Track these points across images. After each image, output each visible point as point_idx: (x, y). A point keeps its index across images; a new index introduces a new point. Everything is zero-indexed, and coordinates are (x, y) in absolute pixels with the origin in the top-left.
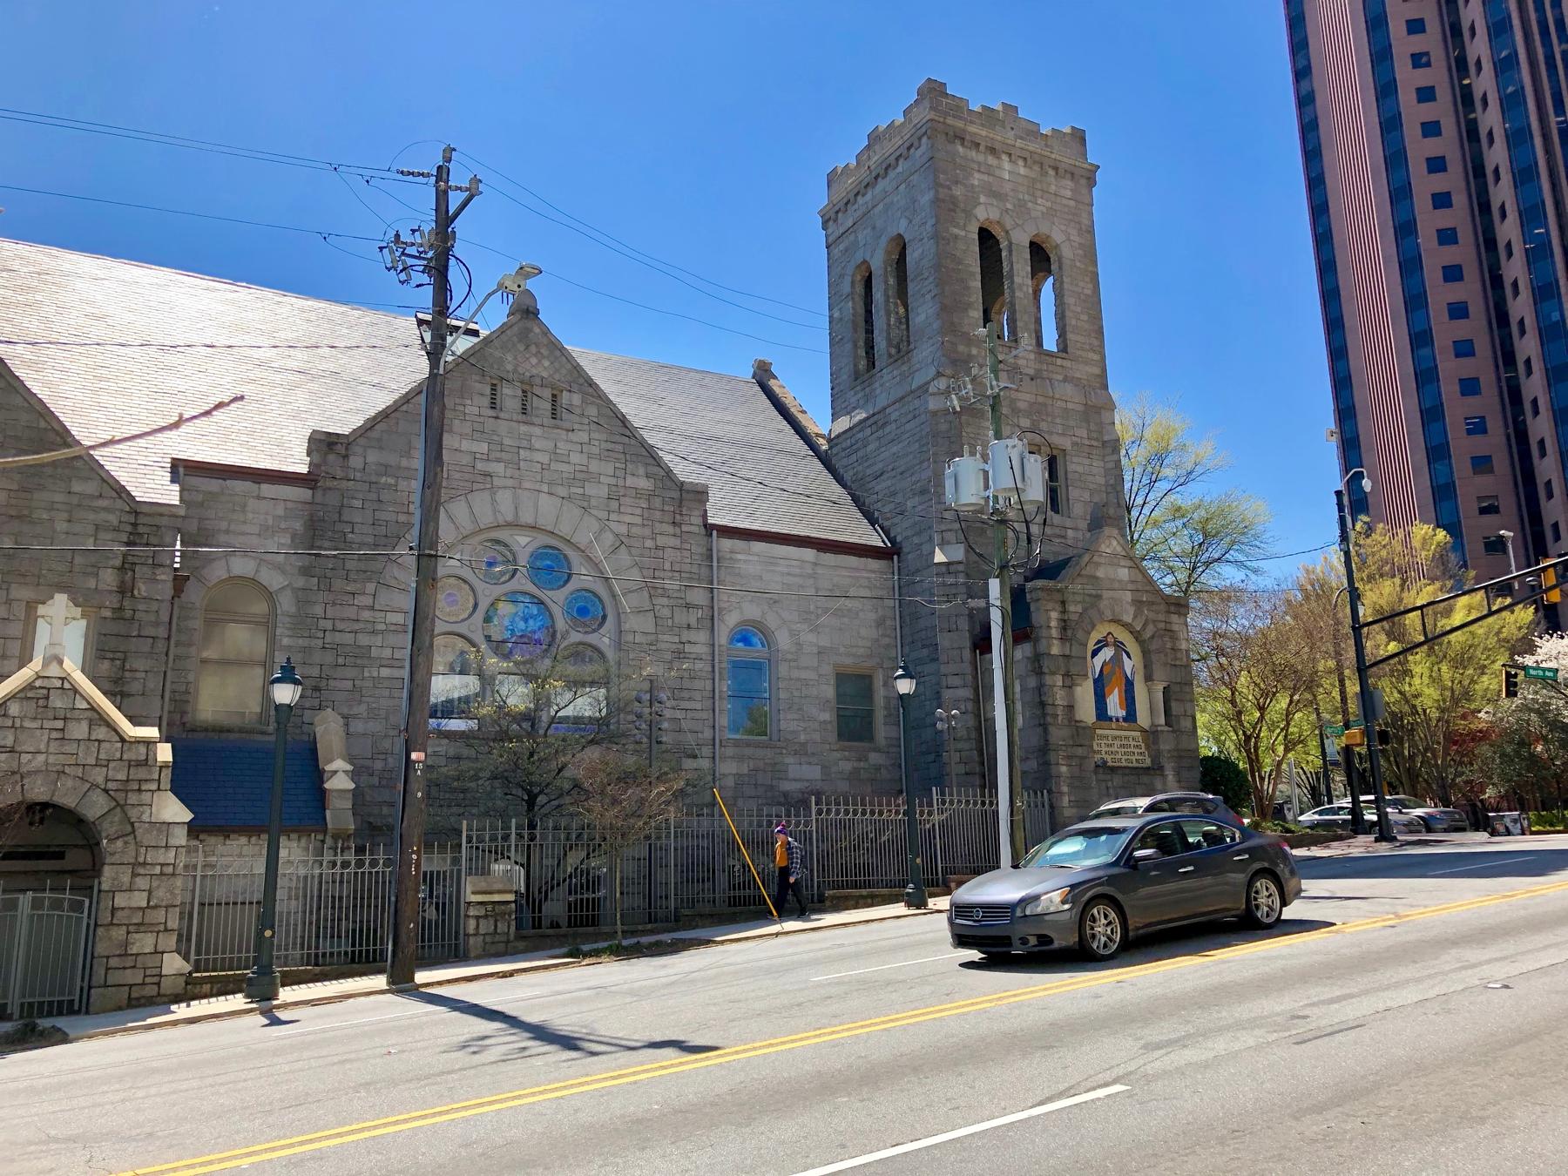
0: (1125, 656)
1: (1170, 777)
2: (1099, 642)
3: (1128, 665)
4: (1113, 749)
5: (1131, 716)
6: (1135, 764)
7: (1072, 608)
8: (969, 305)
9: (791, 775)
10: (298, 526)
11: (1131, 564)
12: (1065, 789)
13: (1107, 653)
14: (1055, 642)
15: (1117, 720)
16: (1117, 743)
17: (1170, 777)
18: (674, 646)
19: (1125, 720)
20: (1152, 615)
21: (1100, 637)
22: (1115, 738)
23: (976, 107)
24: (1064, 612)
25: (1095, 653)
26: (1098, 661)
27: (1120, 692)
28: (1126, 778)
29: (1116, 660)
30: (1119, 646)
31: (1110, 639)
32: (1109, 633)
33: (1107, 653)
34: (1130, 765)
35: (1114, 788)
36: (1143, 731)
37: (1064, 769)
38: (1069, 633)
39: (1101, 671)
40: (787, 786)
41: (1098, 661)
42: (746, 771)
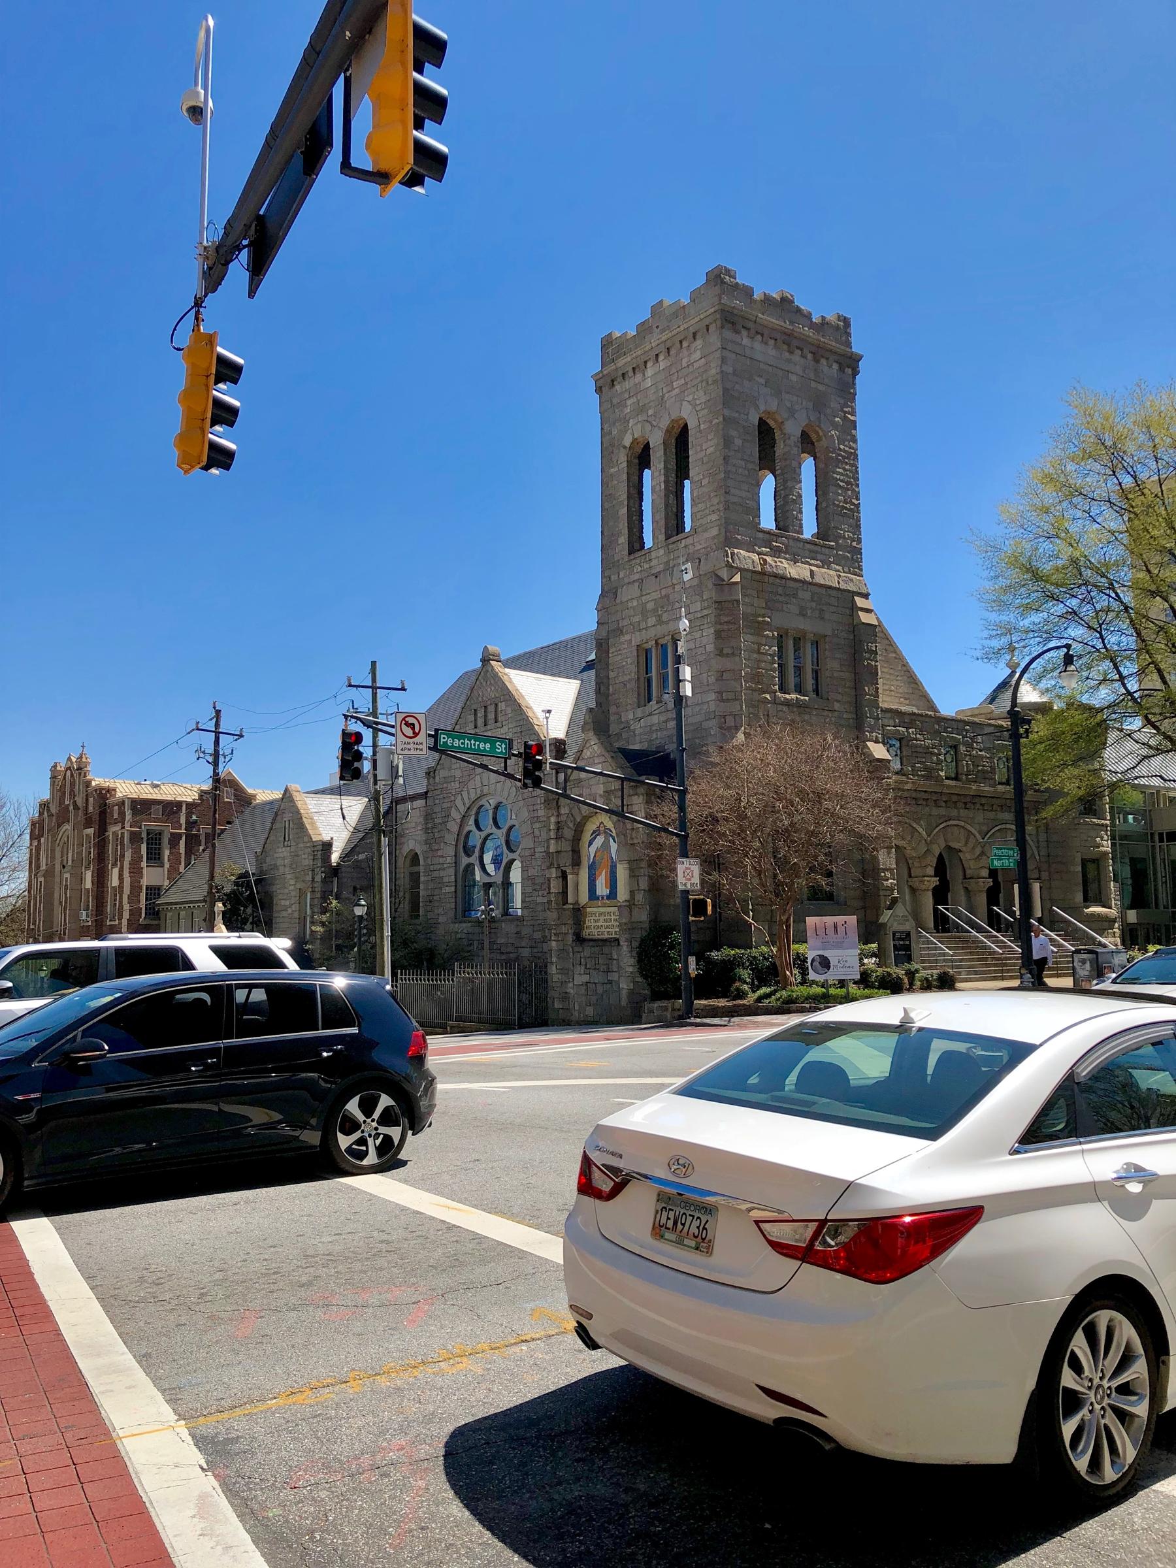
1: (625, 948)
2: (594, 832)
5: (613, 895)
8: (619, 534)
10: (421, 819)
11: (603, 759)
12: (554, 959)
13: (599, 841)
14: (552, 841)
15: (603, 898)
16: (602, 918)
17: (625, 948)
18: (542, 854)
19: (608, 897)
21: (594, 827)
22: (601, 914)
25: (590, 844)
27: (606, 872)
29: (606, 846)
32: (602, 822)
35: (585, 957)
37: (554, 944)
39: (595, 856)
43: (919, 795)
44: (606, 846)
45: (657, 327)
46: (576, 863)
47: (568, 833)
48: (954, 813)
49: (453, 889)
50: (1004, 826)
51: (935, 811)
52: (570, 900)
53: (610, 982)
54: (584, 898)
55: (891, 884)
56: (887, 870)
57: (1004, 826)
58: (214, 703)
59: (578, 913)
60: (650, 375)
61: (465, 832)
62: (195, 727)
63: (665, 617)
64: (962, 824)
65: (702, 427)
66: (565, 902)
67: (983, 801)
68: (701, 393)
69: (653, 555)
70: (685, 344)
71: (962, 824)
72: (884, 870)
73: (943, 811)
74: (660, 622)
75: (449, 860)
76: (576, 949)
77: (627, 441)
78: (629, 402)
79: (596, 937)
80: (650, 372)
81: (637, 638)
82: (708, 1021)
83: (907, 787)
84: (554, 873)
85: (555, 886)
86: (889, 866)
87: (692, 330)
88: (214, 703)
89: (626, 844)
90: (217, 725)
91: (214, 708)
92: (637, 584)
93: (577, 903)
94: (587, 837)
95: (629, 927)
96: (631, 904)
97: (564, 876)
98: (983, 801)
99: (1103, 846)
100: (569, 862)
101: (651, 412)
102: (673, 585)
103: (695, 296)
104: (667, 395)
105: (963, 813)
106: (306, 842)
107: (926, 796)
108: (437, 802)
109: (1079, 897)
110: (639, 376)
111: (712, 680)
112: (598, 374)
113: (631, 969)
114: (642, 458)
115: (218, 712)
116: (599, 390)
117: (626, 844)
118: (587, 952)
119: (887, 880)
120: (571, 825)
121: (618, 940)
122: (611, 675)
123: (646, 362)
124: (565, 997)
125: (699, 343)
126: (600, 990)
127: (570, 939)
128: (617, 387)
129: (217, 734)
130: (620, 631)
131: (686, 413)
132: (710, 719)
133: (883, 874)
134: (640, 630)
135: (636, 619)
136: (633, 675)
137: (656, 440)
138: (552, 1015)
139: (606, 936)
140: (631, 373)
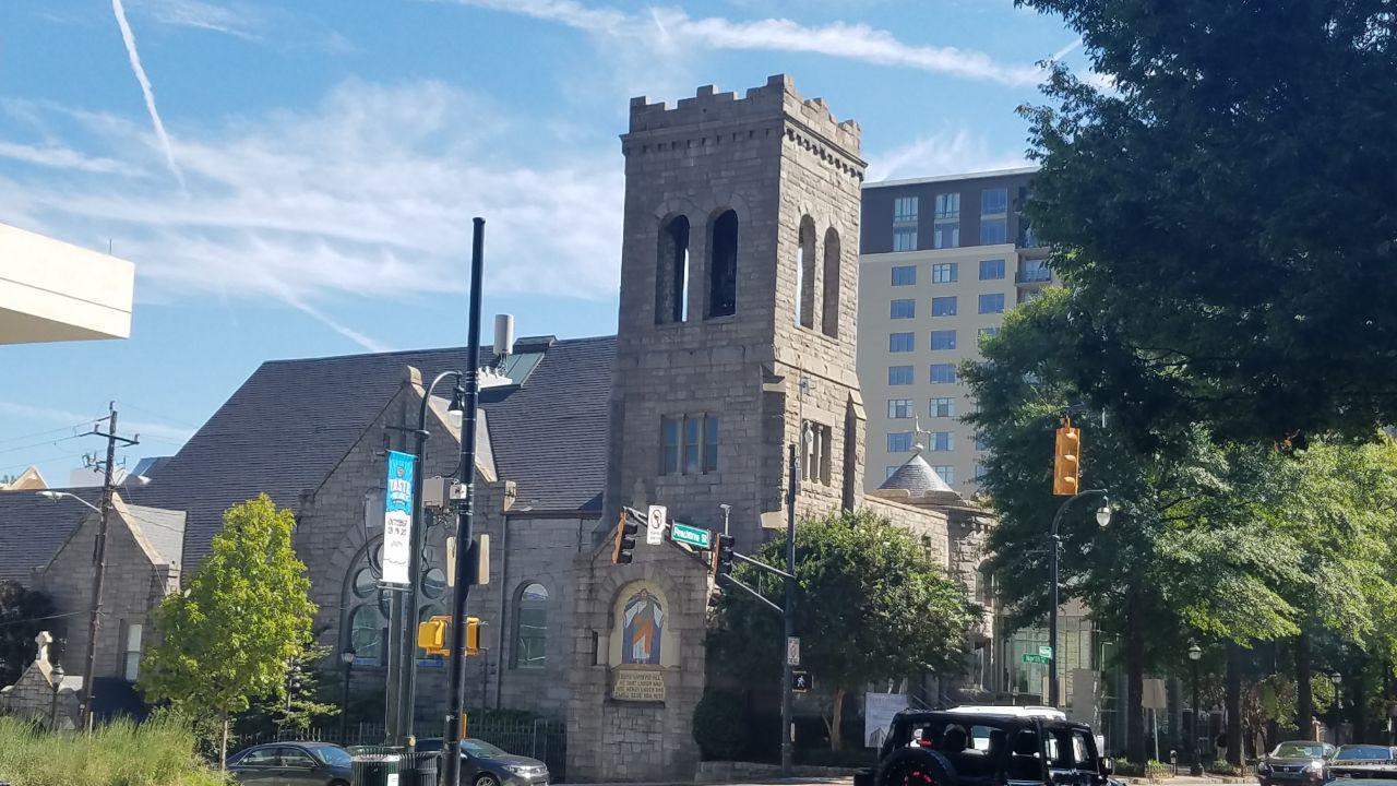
0: (656, 607)
1: (672, 710)
3: (658, 615)
4: (644, 687)
5: (654, 659)
6: (653, 699)
7: (597, 573)
9: (549, 696)
15: (641, 662)
19: (649, 661)
20: (672, 572)
21: (634, 593)
23: (671, 105)
24: (592, 577)
25: (628, 608)
26: (630, 614)
28: (630, 710)
29: (649, 612)
30: (651, 600)
31: (644, 595)
33: (641, 606)
34: (649, 699)
36: (663, 671)
38: (594, 594)
40: (545, 704)
41: (630, 614)
42: (518, 693)
44: (649, 612)
45: (705, 110)
46: (611, 626)
47: (604, 596)
49: (337, 632)
52: (600, 660)
53: (651, 742)
54: (616, 659)
58: (111, 404)
59: (610, 674)
60: (692, 155)
61: (355, 571)
62: (93, 431)
63: (699, 394)
65: (754, 224)
66: (595, 663)
68: (755, 192)
69: (687, 330)
70: (738, 139)
74: (692, 397)
75: (332, 599)
76: (607, 709)
77: (661, 212)
78: (664, 174)
79: (630, 698)
80: (693, 151)
81: (662, 408)
82: (813, 779)
84: (581, 633)
85: (584, 647)
87: (750, 128)
88: (111, 404)
89: (680, 614)
90: (112, 431)
91: (111, 408)
92: (666, 355)
93: (607, 664)
94: (624, 600)
95: (682, 690)
96: (682, 669)
97: (595, 637)
100: (604, 624)
101: (691, 192)
102: (711, 365)
103: (752, 93)
104: (712, 181)
106: (136, 564)
108: (316, 531)
110: (678, 154)
111: (759, 463)
112: (625, 135)
113: (678, 731)
114: (677, 230)
115: (114, 413)
116: (626, 151)
117: (680, 614)
118: (623, 712)
120: (610, 589)
121: (662, 703)
122: (626, 438)
123: (689, 142)
124: (590, 755)
125: (756, 143)
126: (637, 749)
127: (600, 699)
128: (650, 155)
129: (112, 439)
130: (641, 397)
131: (735, 204)
132: (747, 500)
134: (666, 401)
135: (664, 389)
136: (655, 442)
137: (698, 221)
138: (569, 773)
139: (643, 698)
140: (669, 147)
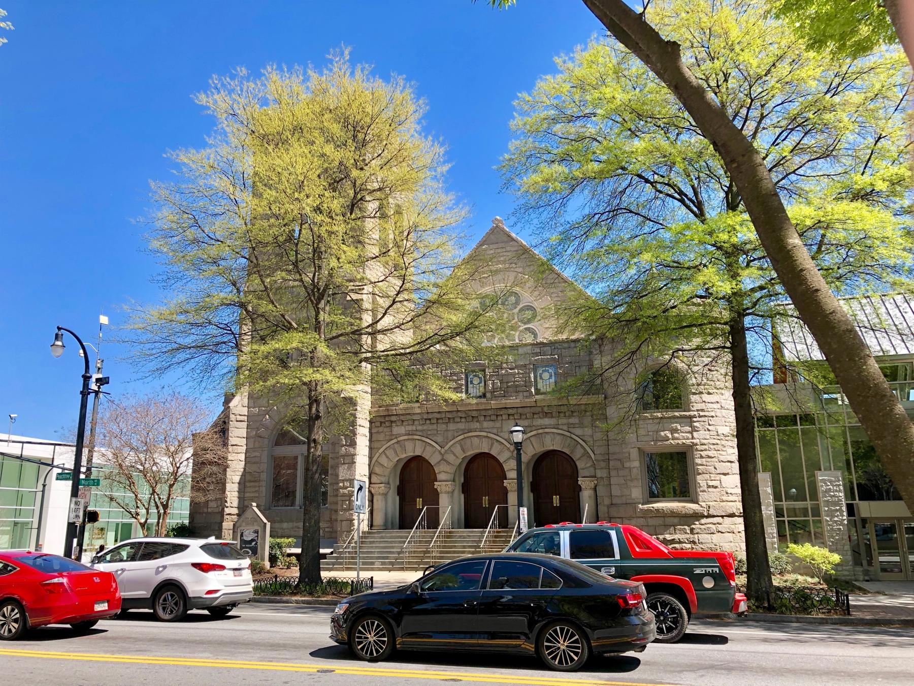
43: (430, 416)
48: (476, 425)
50: (541, 431)
51: (452, 426)
55: (349, 491)
56: (347, 480)
57: (541, 431)
64: (484, 434)
67: (511, 411)
71: (484, 434)
72: (343, 481)
73: (461, 426)
83: (418, 411)
86: (348, 477)
98: (511, 411)
99: (674, 438)
105: (485, 424)
107: (438, 416)
109: (637, 492)
119: (346, 488)
133: (341, 484)
